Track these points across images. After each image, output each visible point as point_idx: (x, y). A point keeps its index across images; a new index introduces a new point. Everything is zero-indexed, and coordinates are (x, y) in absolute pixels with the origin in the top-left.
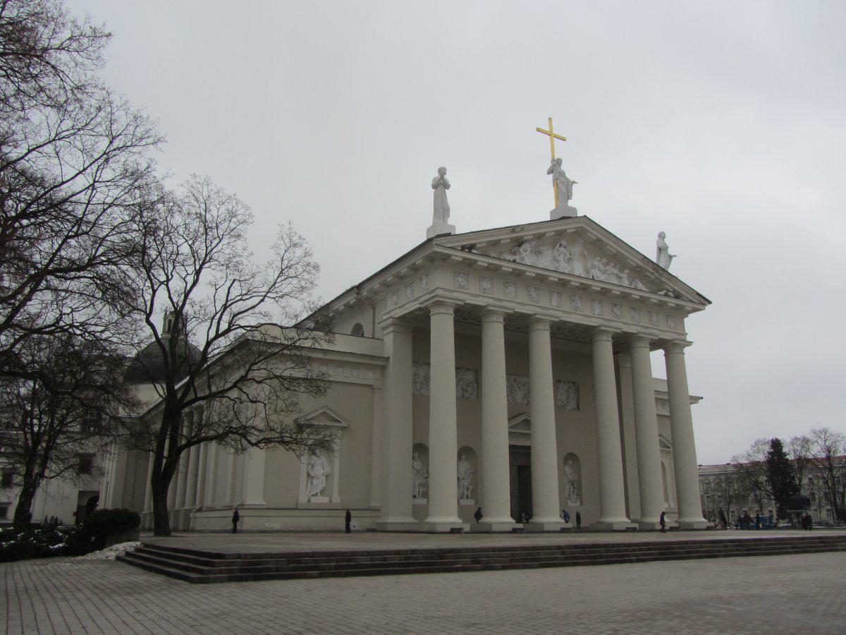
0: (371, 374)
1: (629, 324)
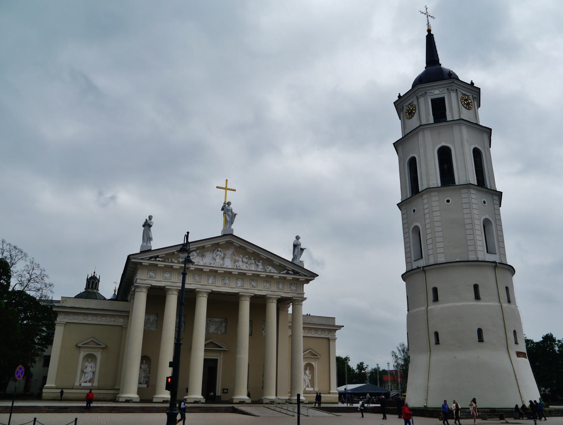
0: (122, 320)
1: (262, 290)
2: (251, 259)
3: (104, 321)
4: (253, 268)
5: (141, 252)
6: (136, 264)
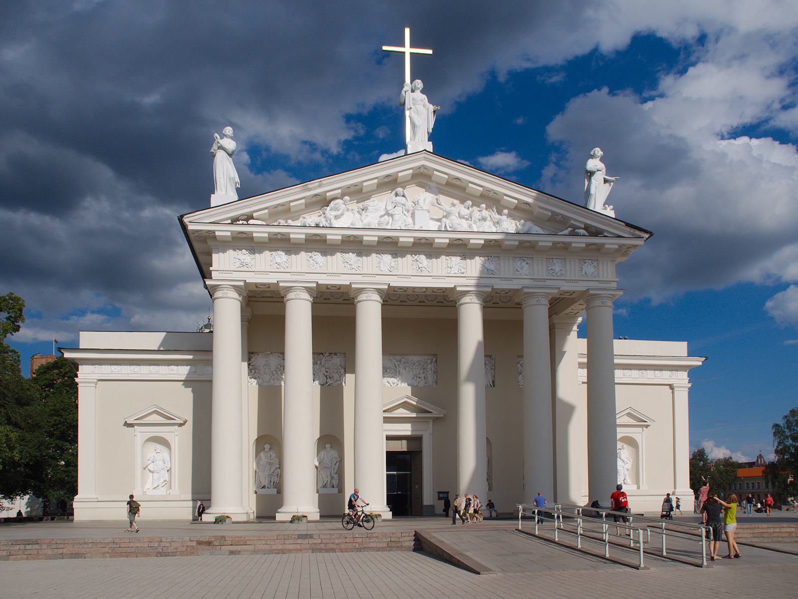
3: (171, 372)
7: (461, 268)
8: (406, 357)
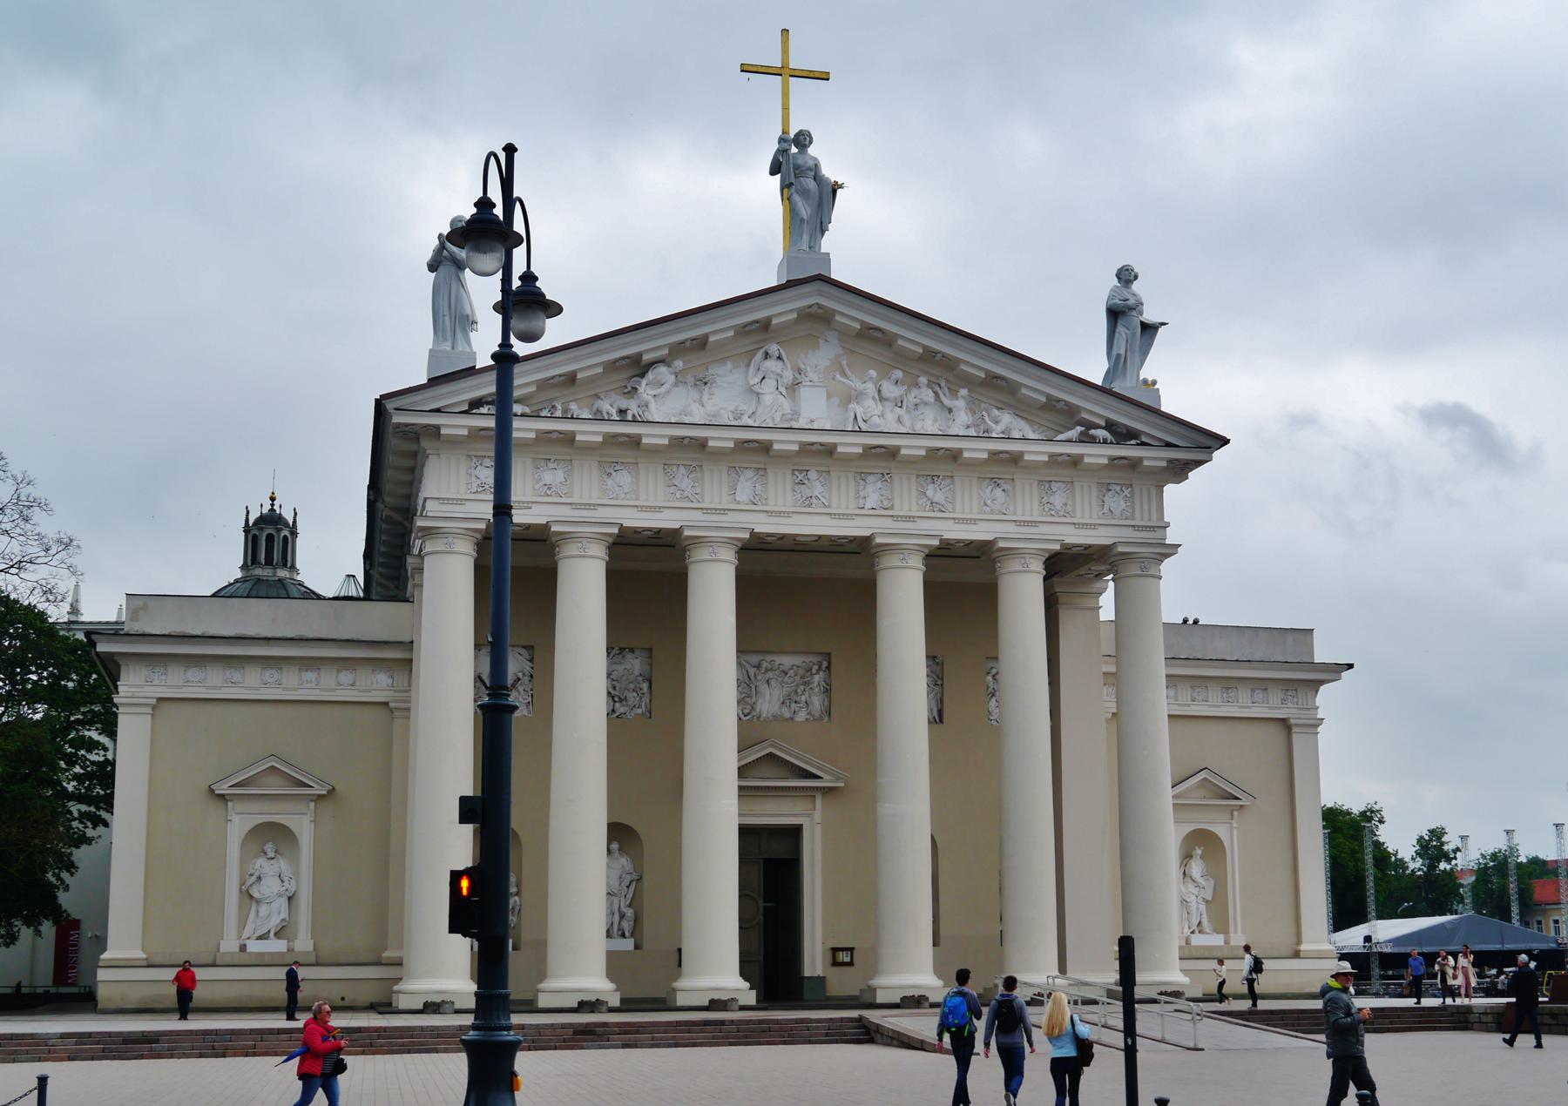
2: (917, 385)
3: (309, 685)
4: (929, 421)
5: (429, 380)
6: (413, 434)
7: (882, 498)
8: (769, 658)
